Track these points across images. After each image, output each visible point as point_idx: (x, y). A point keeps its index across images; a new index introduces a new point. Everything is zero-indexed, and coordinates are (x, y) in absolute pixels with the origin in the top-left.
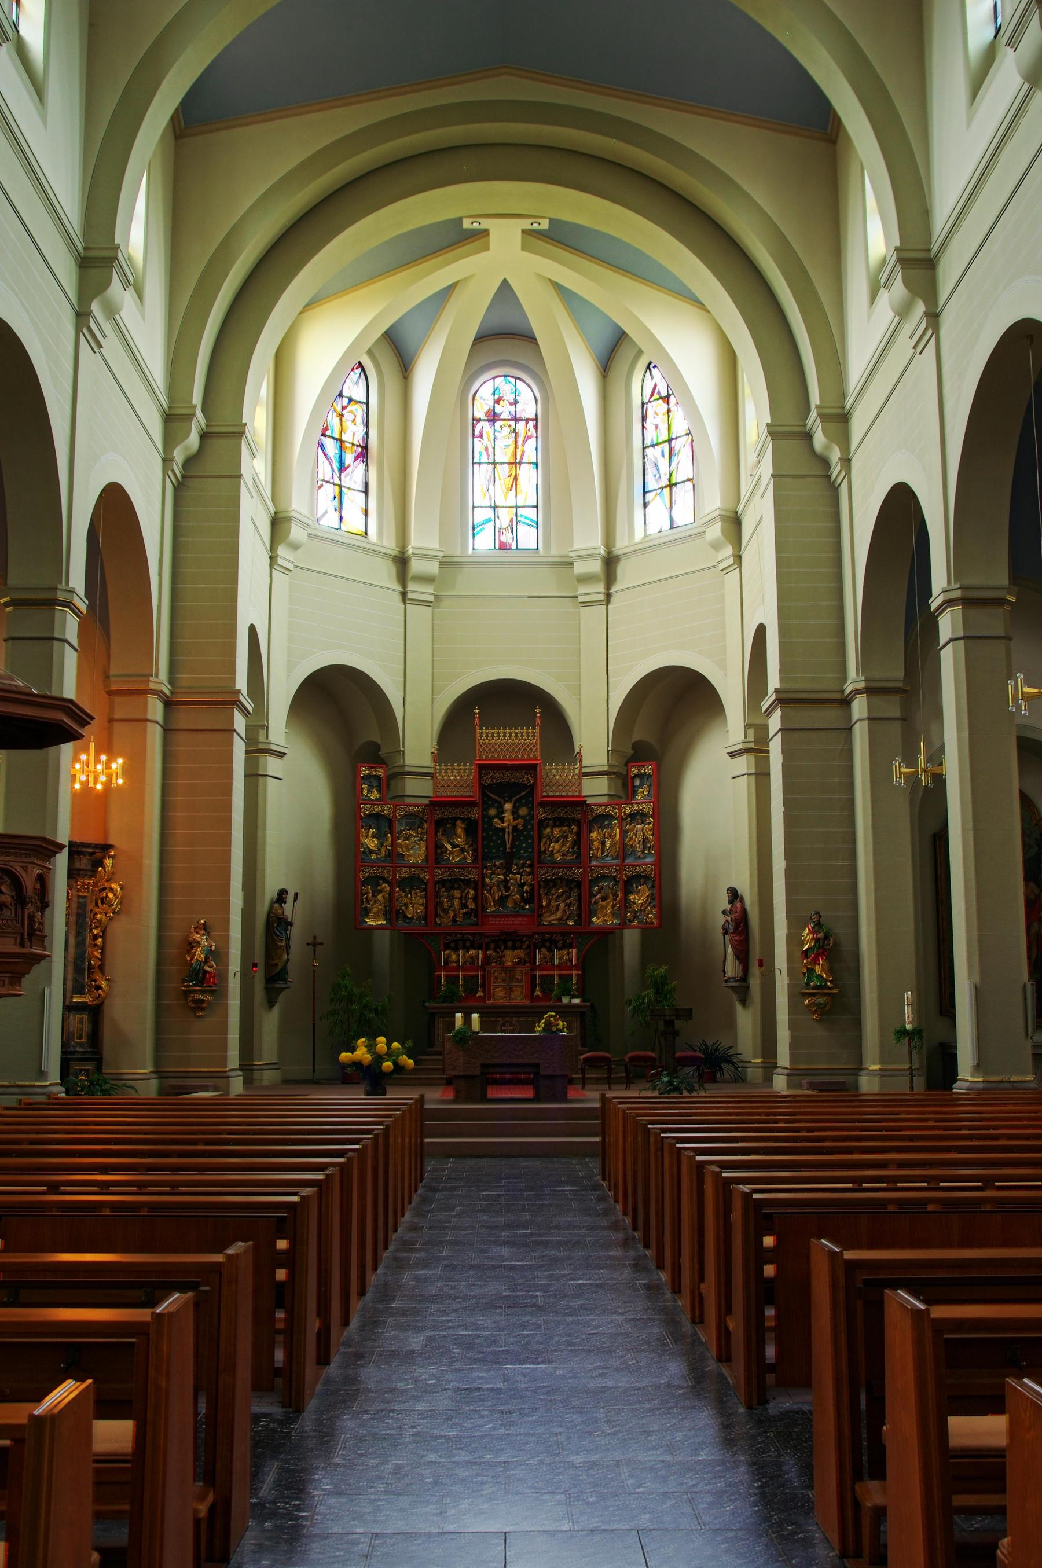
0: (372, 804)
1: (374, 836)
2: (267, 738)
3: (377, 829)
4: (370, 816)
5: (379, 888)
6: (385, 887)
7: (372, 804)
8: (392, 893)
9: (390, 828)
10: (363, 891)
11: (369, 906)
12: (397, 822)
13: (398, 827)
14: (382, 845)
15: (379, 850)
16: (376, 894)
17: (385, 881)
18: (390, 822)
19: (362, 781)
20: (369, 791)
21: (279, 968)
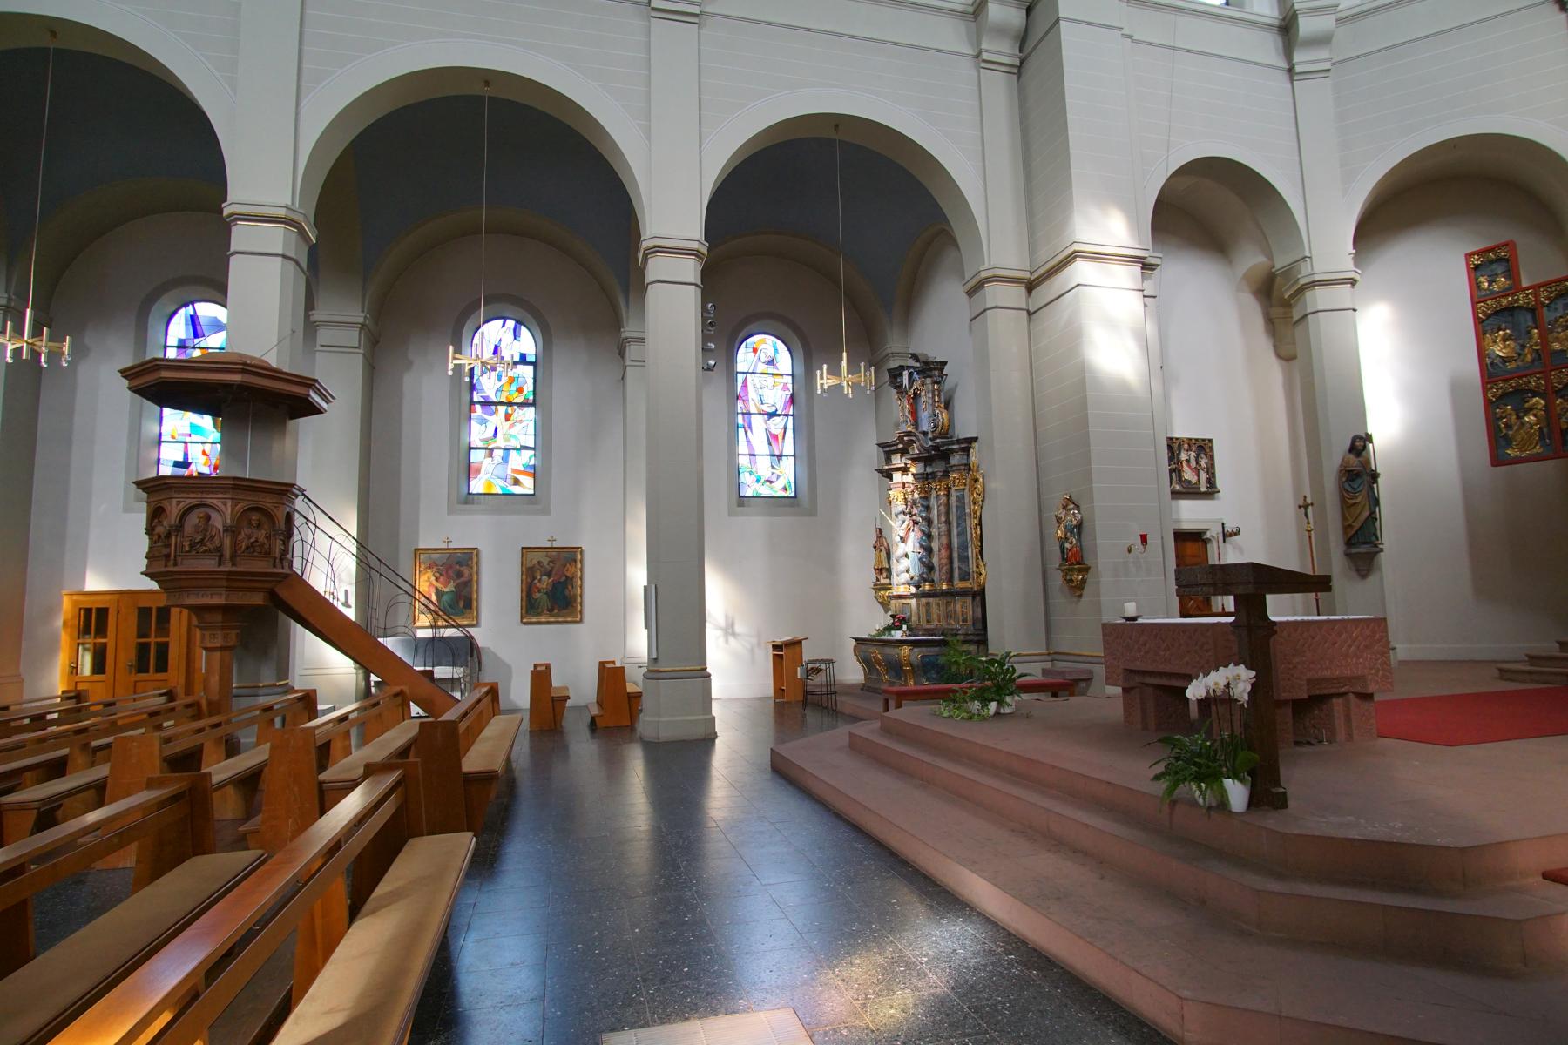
0: (1495, 298)
1: (1505, 339)
2: (1312, 269)
3: (1513, 329)
4: (1496, 313)
5: (1527, 405)
6: (1537, 403)
7: (1495, 298)
8: (1547, 408)
9: (1535, 321)
10: (1498, 416)
11: (1510, 433)
12: (1545, 309)
13: (1548, 315)
14: (1523, 347)
15: (1520, 355)
16: (1521, 414)
17: (1535, 394)
18: (1532, 311)
19: (1478, 273)
20: (1490, 283)
21: (1355, 529)
